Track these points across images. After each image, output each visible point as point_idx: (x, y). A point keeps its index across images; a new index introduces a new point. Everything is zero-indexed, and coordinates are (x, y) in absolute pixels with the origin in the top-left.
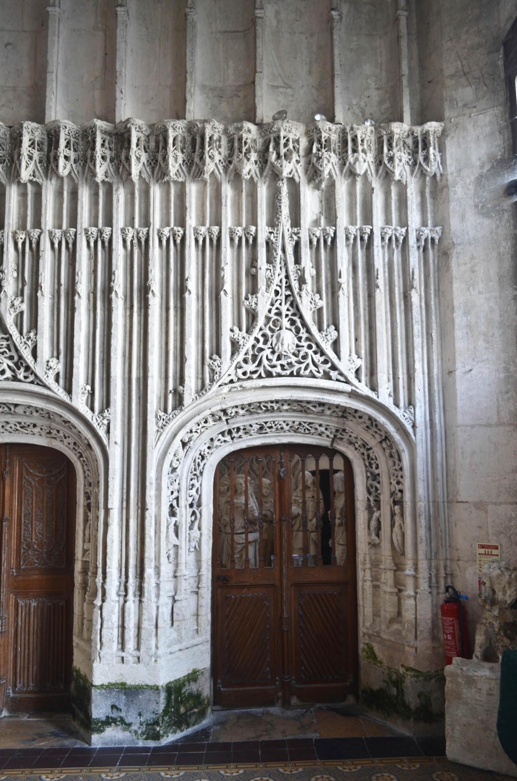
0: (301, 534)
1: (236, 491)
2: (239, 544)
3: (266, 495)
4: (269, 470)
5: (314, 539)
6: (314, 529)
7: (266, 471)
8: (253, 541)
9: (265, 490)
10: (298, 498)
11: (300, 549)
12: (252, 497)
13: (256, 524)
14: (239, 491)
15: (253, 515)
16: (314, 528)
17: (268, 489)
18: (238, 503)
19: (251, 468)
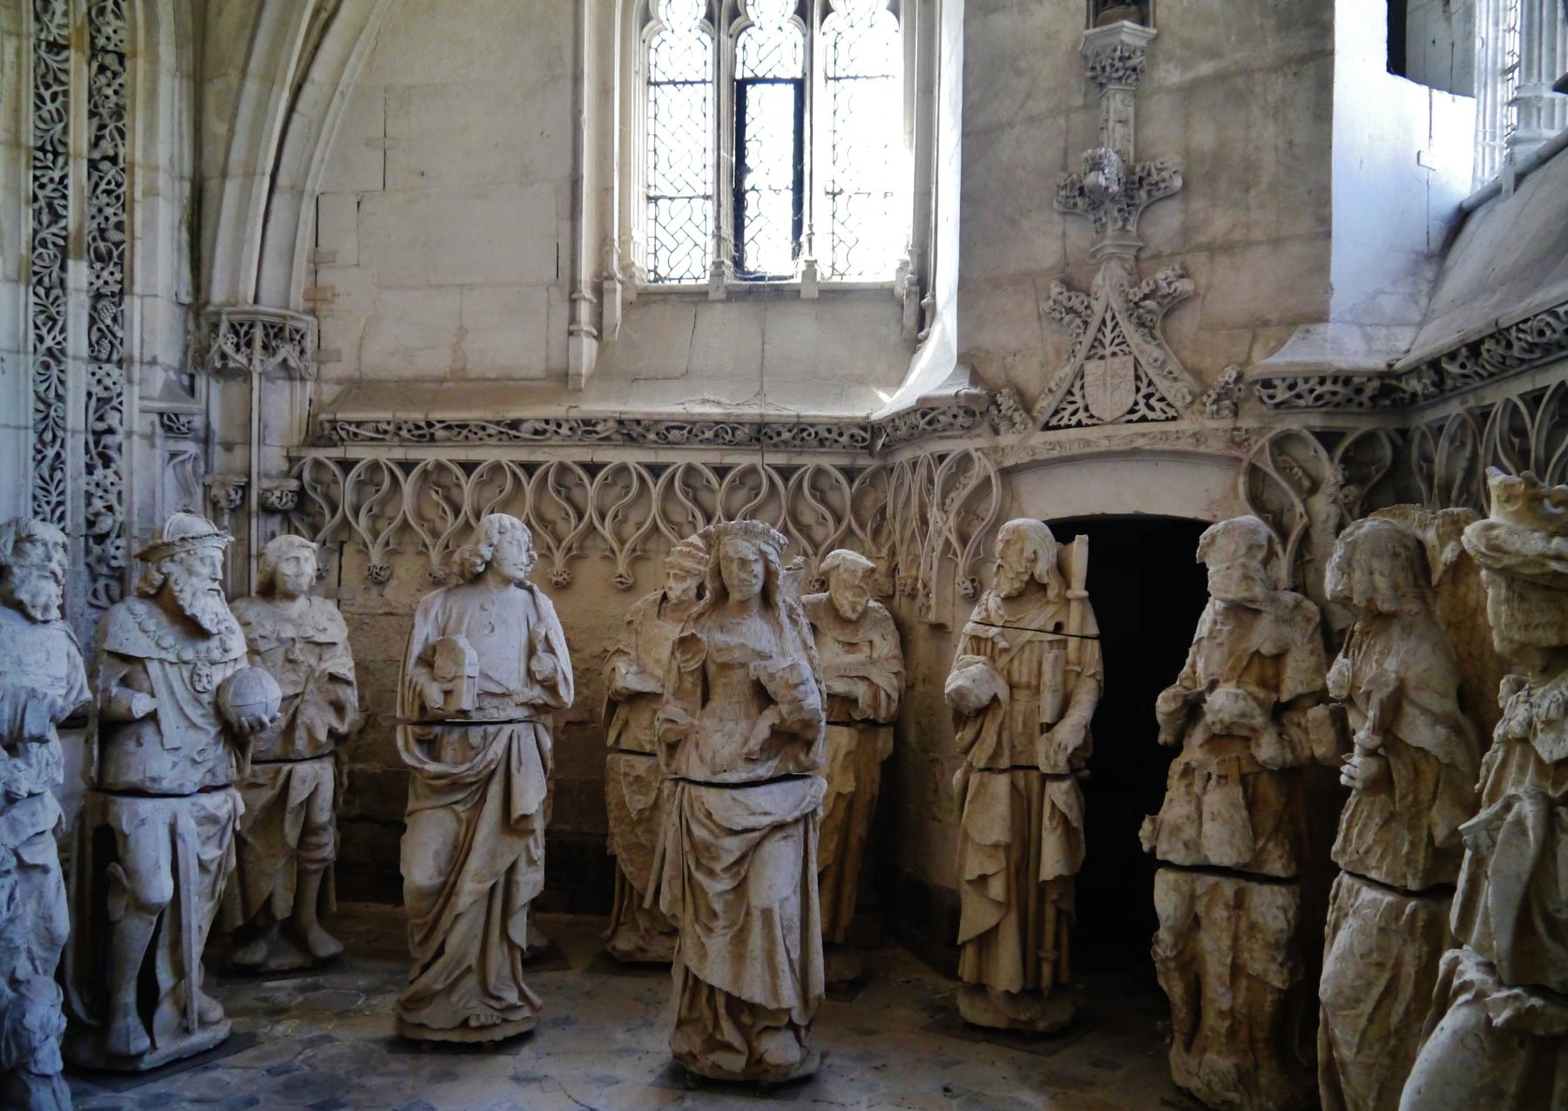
0: (1001, 784)
1: (723, 594)
2: (733, 833)
3: (854, 617)
4: (862, 526)
5: (1061, 805)
6: (1063, 767)
7: (850, 531)
8: (796, 821)
9: (849, 595)
10: (993, 631)
11: (996, 846)
12: (794, 622)
13: (809, 744)
14: (735, 596)
15: (797, 704)
16: (1062, 761)
17: (860, 591)
18: (729, 648)
19: (794, 515)
